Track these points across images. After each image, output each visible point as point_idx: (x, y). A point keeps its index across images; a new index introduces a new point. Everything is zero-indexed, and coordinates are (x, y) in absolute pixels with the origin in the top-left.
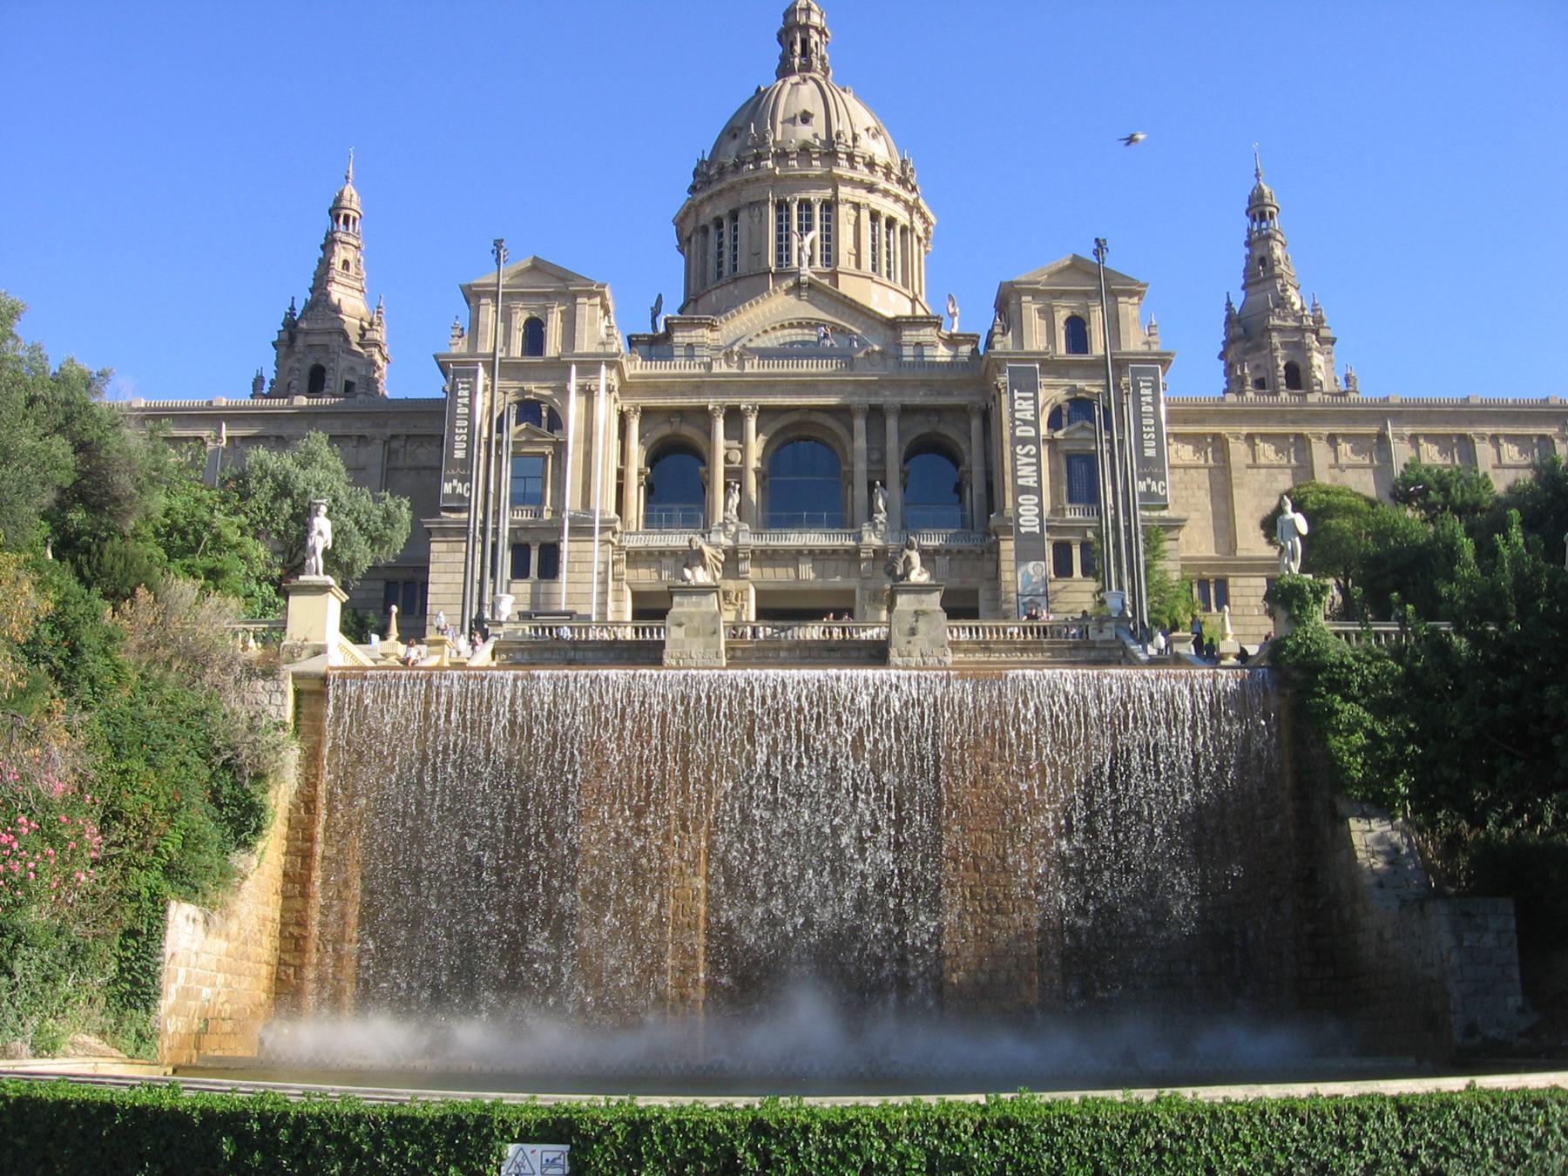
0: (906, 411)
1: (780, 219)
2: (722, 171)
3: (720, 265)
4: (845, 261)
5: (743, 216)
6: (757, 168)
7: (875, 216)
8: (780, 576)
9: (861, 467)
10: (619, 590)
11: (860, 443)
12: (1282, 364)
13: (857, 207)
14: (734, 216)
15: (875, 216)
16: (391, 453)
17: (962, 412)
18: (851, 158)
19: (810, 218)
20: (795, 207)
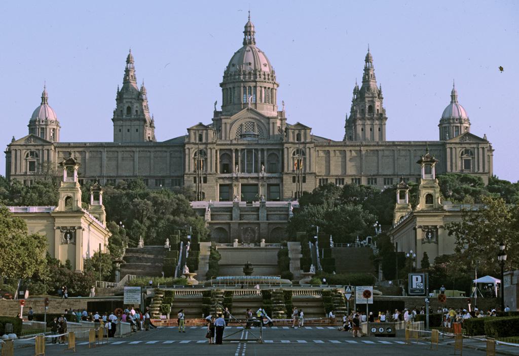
0: (268, 150)
1: (244, 90)
2: (231, 75)
3: (231, 98)
4: (258, 101)
5: (236, 89)
6: (239, 78)
7: (265, 88)
8: (245, 181)
9: (260, 160)
10: (217, 184)
11: (260, 156)
12: (367, 107)
13: (261, 87)
14: (234, 88)
15: (265, 88)
16: (171, 154)
17: (278, 150)
18: (260, 75)
19: (251, 90)
20: (247, 88)
